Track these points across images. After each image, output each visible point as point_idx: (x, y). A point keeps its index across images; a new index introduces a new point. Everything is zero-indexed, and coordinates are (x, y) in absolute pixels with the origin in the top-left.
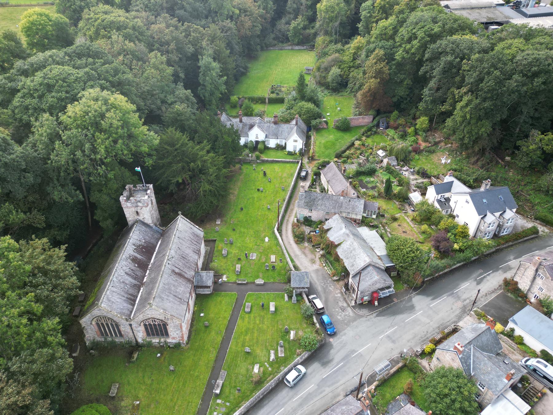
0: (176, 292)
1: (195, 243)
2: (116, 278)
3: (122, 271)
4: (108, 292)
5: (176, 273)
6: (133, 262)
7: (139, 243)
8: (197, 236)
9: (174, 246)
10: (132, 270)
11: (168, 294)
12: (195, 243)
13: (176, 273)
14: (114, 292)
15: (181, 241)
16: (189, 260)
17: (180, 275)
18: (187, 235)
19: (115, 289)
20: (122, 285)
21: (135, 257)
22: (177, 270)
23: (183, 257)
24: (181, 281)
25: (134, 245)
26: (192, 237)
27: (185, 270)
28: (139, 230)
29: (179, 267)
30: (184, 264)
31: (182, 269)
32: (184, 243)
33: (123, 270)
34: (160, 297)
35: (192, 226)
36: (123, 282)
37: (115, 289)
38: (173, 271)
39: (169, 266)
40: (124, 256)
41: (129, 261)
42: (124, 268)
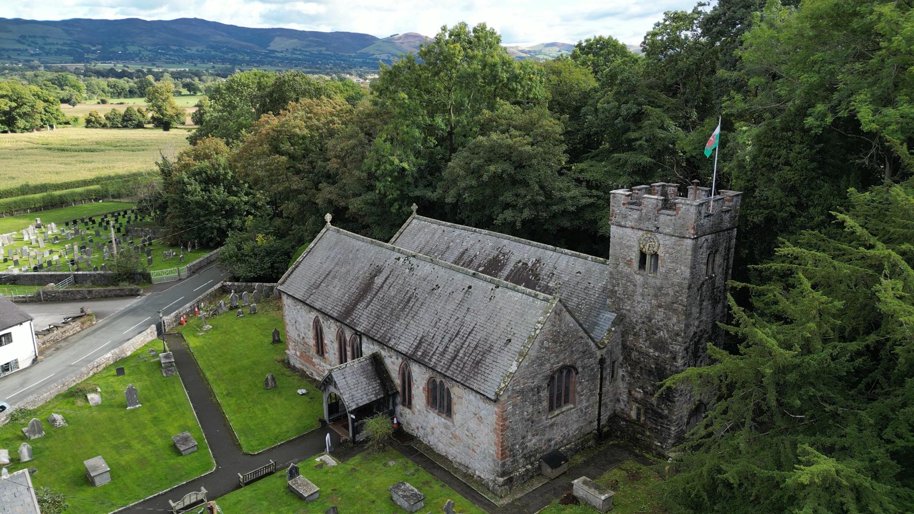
0: (334, 277)
1: (451, 349)
2: (459, 235)
3: (471, 242)
4: (435, 226)
5: (373, 277)
6: (490, 261)
7: (544, 272)
8: (477, 363)
9: (442, 272)
10: (471, 261)
11: (336, 260)
12: (451, 349)
13: (373, 277)
14: (434, 234)
15: (459, 296)
16: (398, 319)
17: (366, 288)
18: (482, 319)
19: (437, 236)
20: (442, 247)
21: (504, 265)
22: (378, 281)
23: (407, 303)
24: (354, 290)
25: (538, 261)
26: (472, 341)
27: (375, 305)
28: (588, 271)
29: (385, 287)
30: (390, 302)
31: (380, 295)
32: (451, 306)
33: (472, 245)
34: (336, 244)
35: (516, 346)
36: (448, 248)
37: (437, 236)
38: (379, 271)
39: (391, 261)
40: (506, 242)
41: (495, 253)
42: (478, 246)
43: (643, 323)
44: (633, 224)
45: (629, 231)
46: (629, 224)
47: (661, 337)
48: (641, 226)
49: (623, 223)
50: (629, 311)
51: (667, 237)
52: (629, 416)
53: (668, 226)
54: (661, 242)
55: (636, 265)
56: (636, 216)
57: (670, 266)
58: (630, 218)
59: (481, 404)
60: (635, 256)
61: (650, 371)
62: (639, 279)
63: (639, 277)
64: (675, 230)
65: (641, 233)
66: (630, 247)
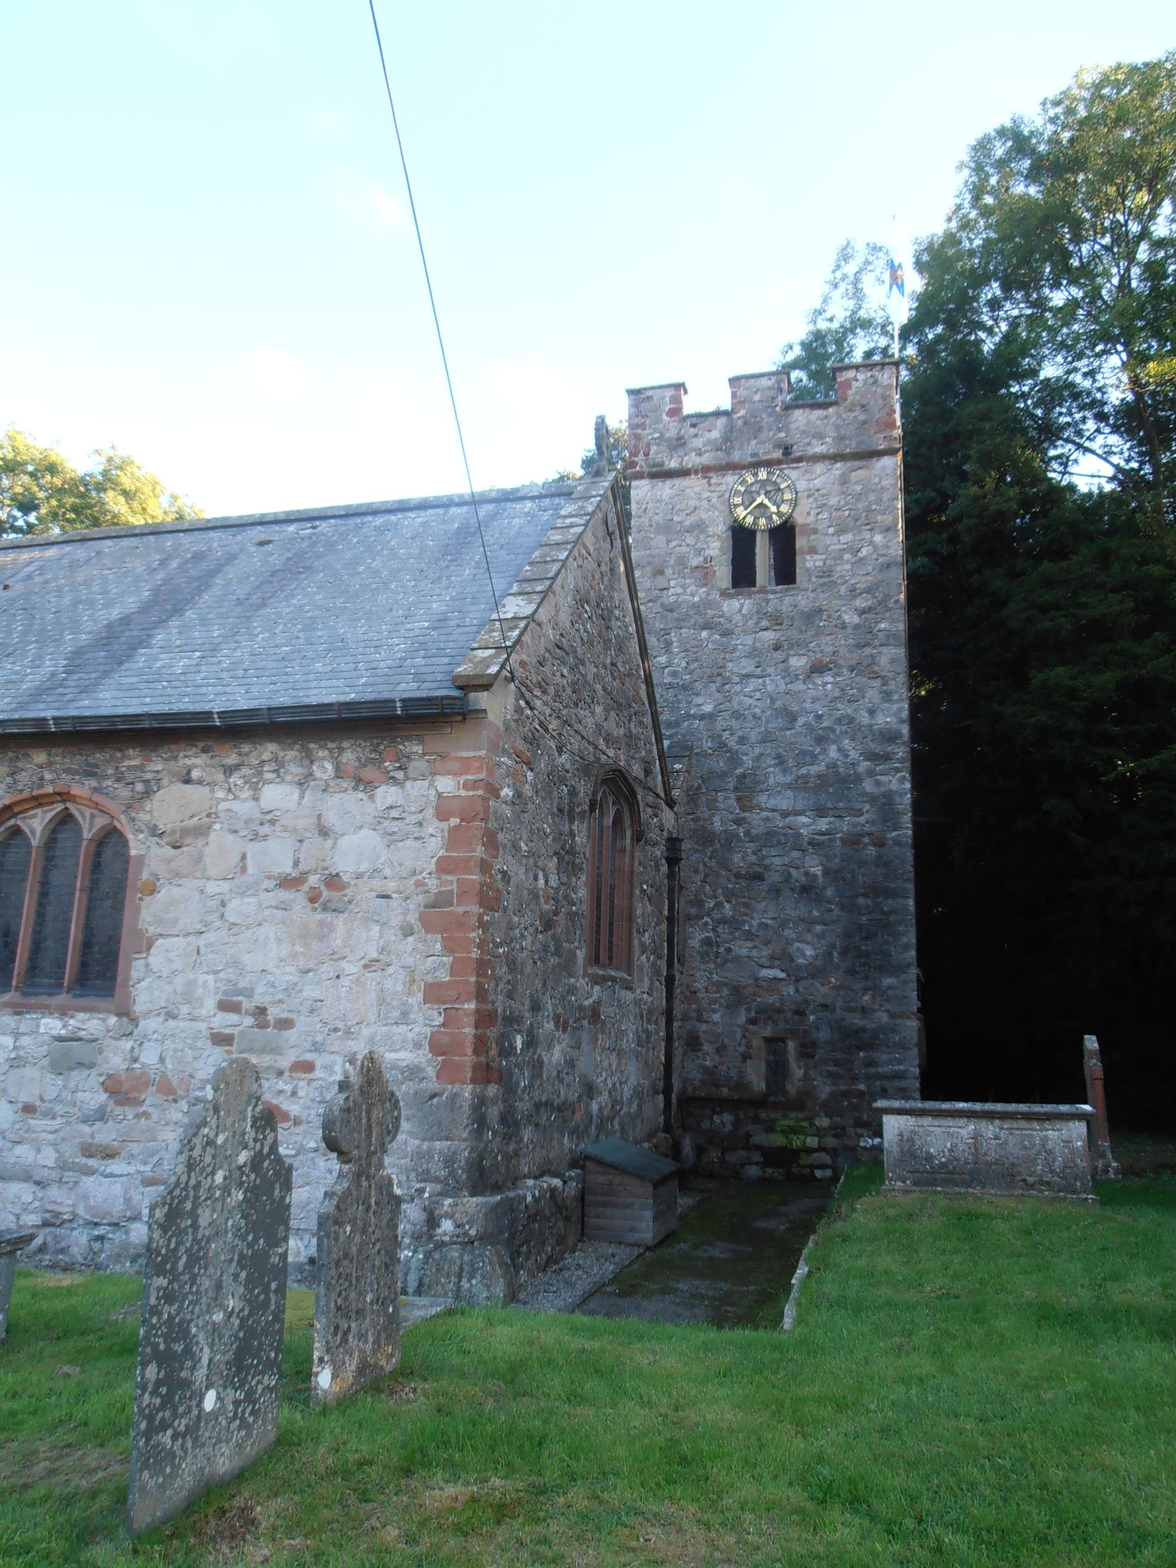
43: (766, 739)
44: (707, 459)
45: (694, 484)
46: (691, 460)
47: (833, 765)
48: (736, 456)
49: (673, 464)
50: (711, 717)
51: (819, 468)
52: (741, 1085)
53: (820, 436)
54: (801, 485)
55: (723, 573)
56: (715, 434)
57: (836, 543)
58: (698, 443)
59: (343, 805)
60: (717, 548)
61: (805, 889)
62: (738, 607)
63: (735, 604)
64: (840, 439)
65: (730, 479)
66: (700, 527)
